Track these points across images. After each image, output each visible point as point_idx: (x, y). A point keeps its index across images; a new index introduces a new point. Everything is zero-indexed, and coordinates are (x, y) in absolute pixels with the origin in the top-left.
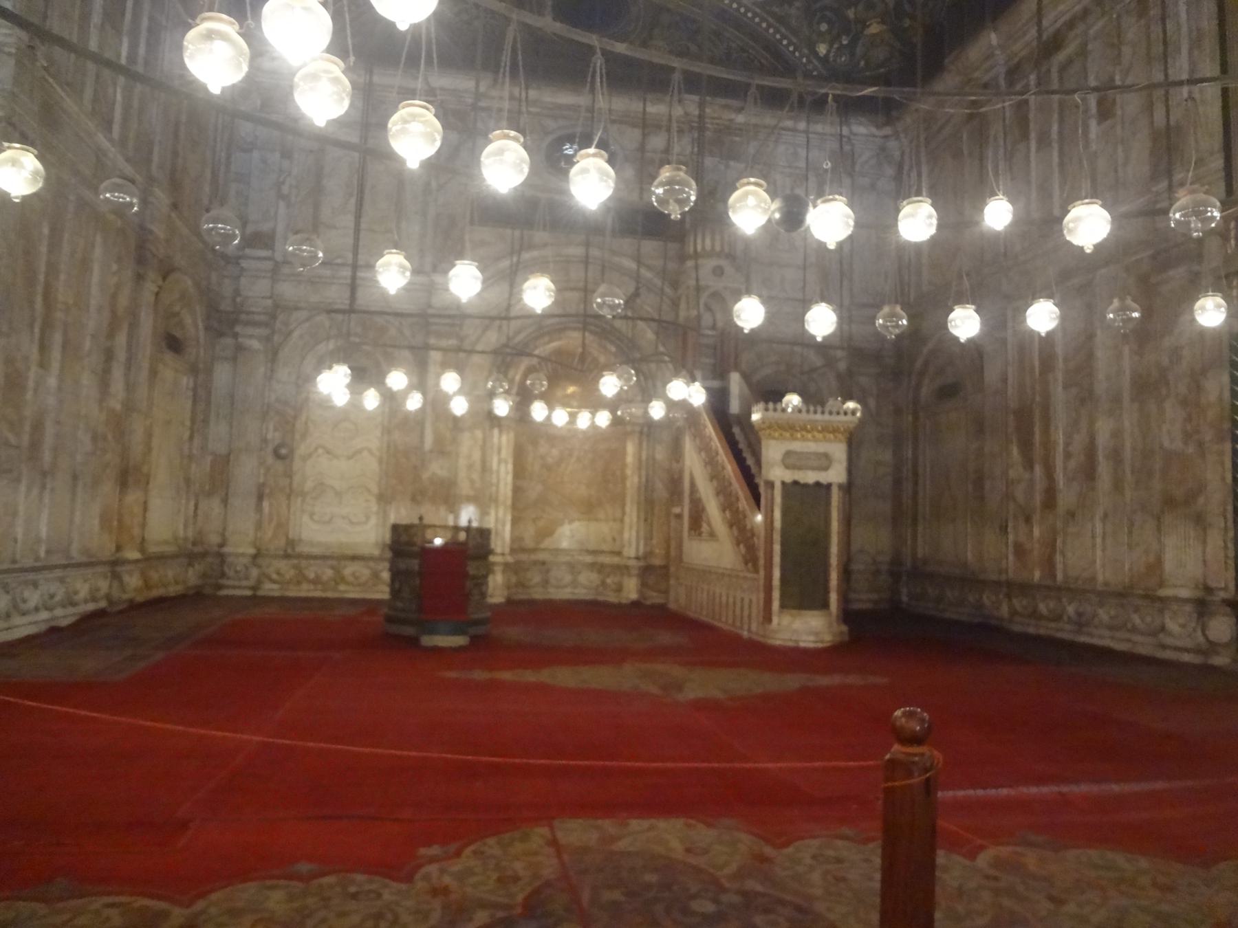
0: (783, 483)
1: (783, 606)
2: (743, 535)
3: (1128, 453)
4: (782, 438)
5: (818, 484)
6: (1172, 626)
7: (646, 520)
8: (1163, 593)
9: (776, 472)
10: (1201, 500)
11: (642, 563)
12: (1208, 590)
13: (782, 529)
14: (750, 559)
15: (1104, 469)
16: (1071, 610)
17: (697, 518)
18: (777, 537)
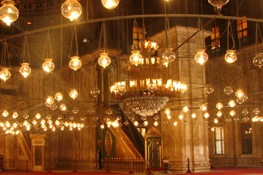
0: (35, 146)
1: (35, 165)
2: (29, 155)
3: (87, 140)
4: (34, 139)
5: (40, 146)
6: (90, 165)
7: (10, 152)
8: (90, 160)
9: (34, 144)
10: (93, 147)
11: (10, 160)
12: (94, 159)
13: (35, 153)
14: (30, 158)
15: (85, 142)
16: (82, 164)
17: (21, 151)
18: (34, 154)
